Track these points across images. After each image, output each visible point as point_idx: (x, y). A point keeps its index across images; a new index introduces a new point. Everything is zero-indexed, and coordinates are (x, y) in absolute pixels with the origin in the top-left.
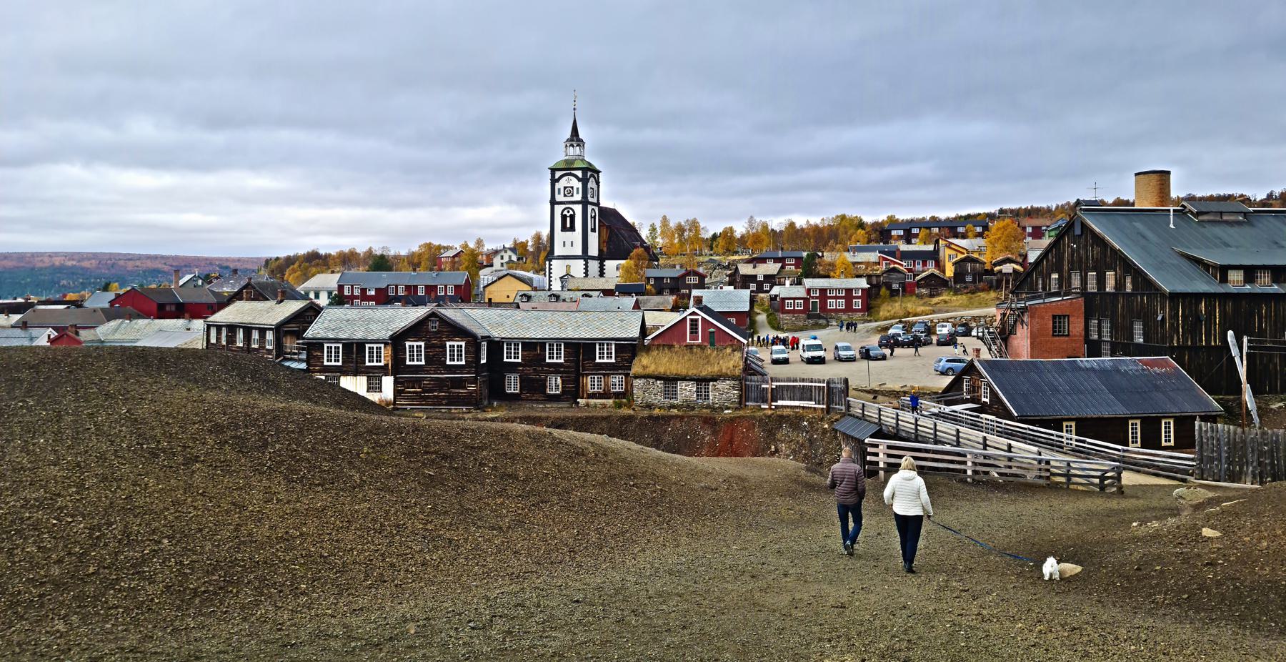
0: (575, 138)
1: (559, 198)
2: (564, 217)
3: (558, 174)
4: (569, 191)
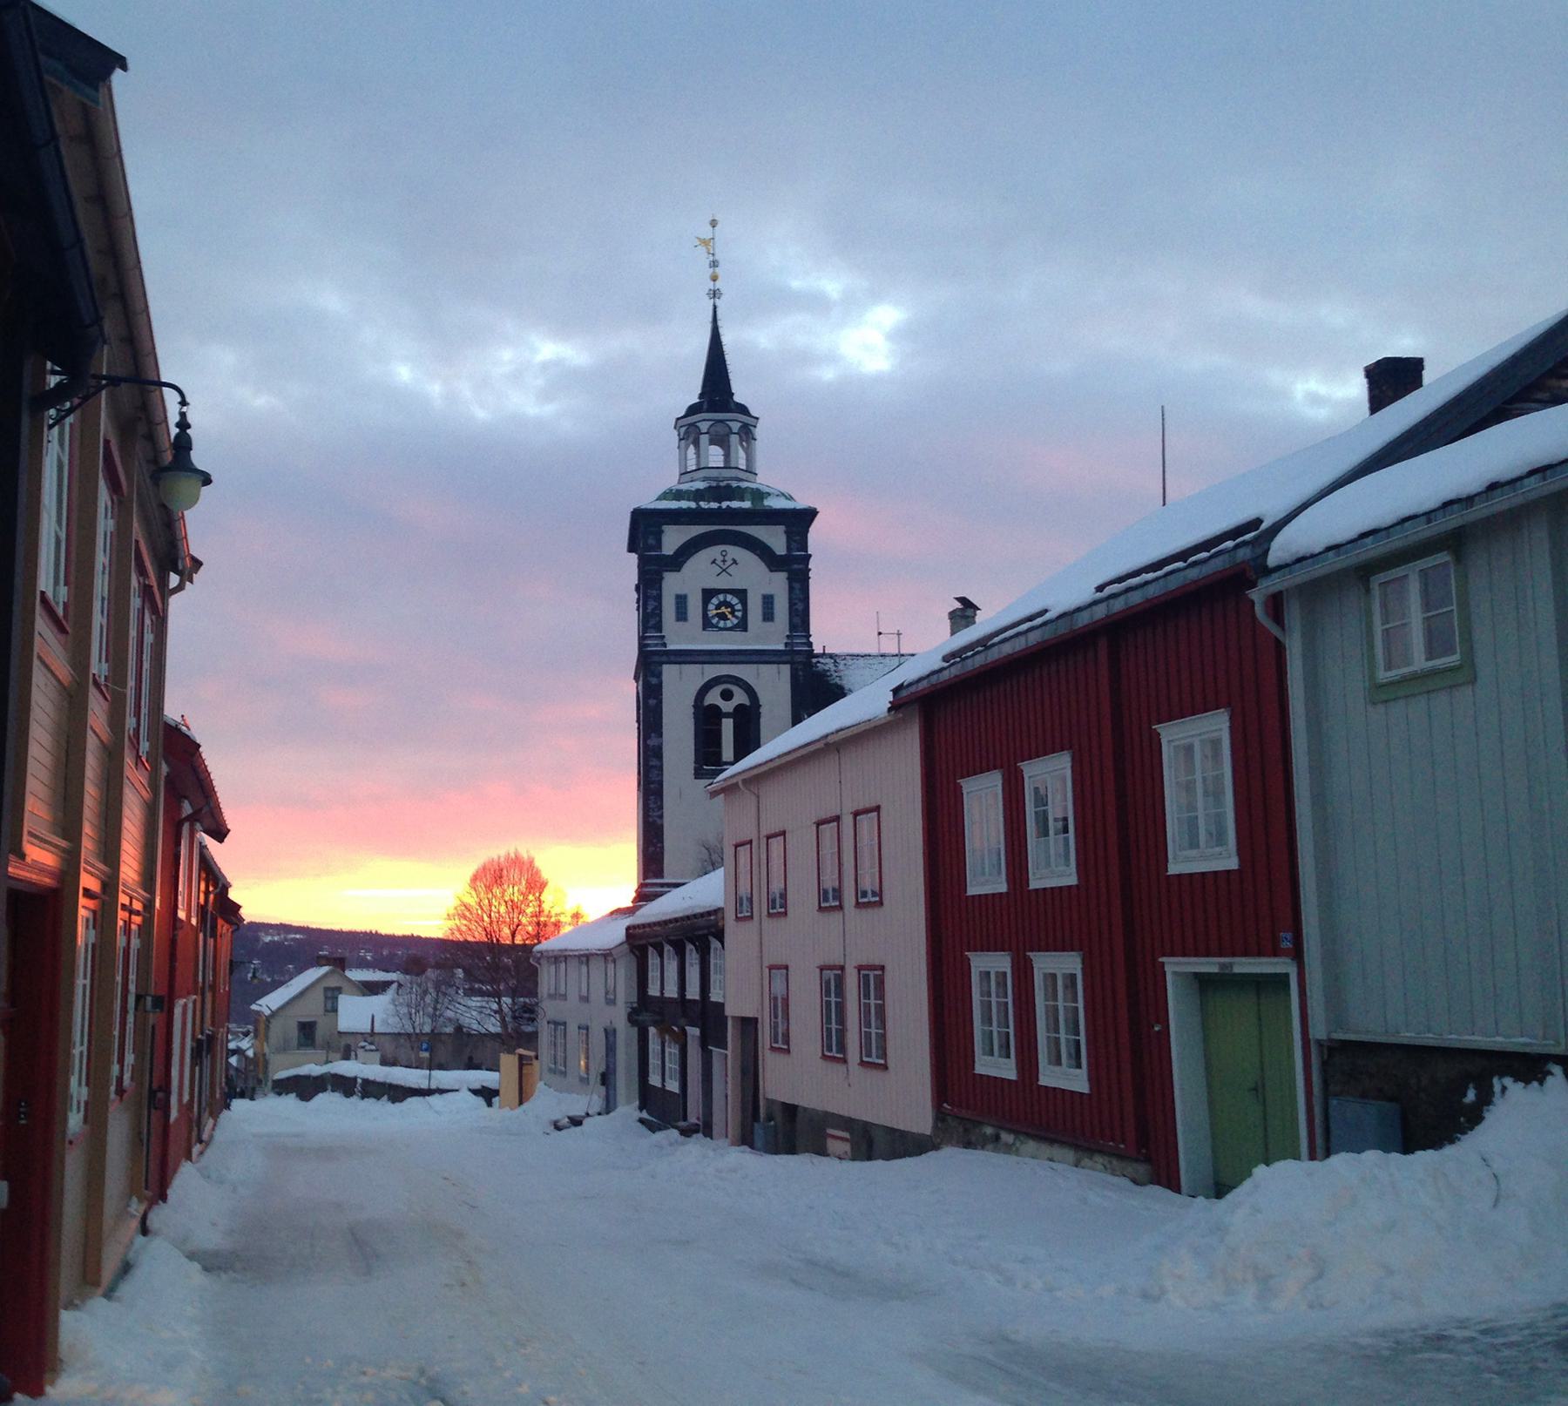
1: (679, 636)
2: (706, 720)
4: (724, 606)
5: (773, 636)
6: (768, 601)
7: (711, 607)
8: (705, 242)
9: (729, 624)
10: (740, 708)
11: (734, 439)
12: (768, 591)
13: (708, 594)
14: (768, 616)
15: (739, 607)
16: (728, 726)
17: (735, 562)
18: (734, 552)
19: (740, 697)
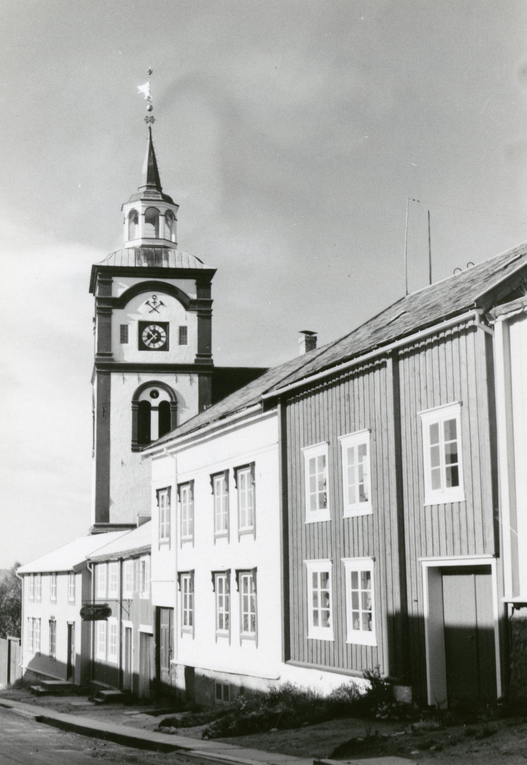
2: (141, 411)
3: (120, 286)
6: (183, 331)
7: (145, 334)
9: (157, 346)
11: (161, 219)
12: (183, 324)
13: (143, 325)
14: (182, 340)
15: (163, 334)
16: (155, 416)
17: (162, 303)
19: (164, 396)
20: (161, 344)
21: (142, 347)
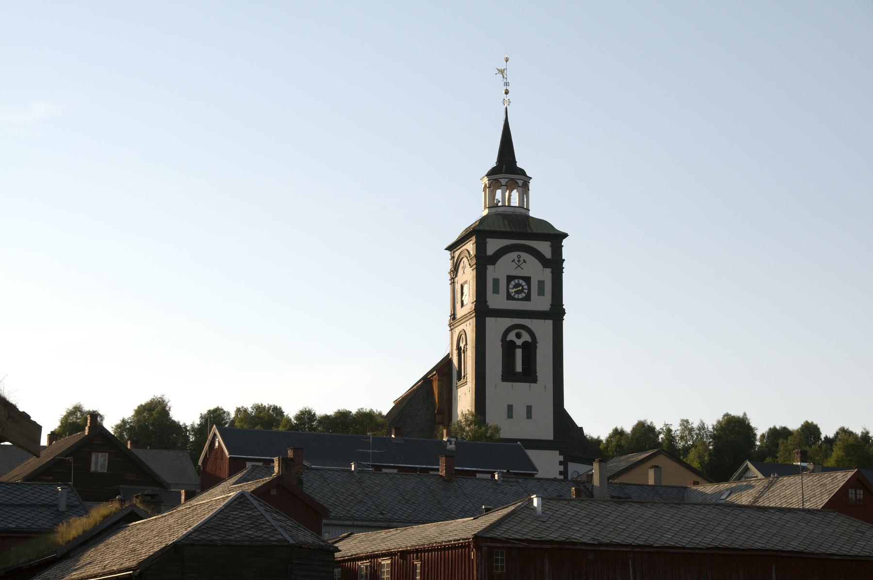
0: (507, 170)
1: (496, 301)
5: (542, 303)
6: (541, 284)
7: (511, 286)
8: (502, 72)
9: (520, 296)
10: (525, 344)
13: (510, 278)
14: (541, 292)
15: (526, 287)
16: (519, 353)
17: (525, 261)
18: (524, 256)
19: (526, 337)
20: (524, 295)
21: (509, 297)
